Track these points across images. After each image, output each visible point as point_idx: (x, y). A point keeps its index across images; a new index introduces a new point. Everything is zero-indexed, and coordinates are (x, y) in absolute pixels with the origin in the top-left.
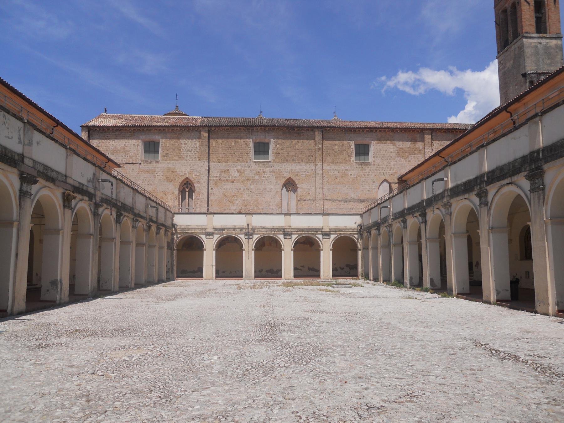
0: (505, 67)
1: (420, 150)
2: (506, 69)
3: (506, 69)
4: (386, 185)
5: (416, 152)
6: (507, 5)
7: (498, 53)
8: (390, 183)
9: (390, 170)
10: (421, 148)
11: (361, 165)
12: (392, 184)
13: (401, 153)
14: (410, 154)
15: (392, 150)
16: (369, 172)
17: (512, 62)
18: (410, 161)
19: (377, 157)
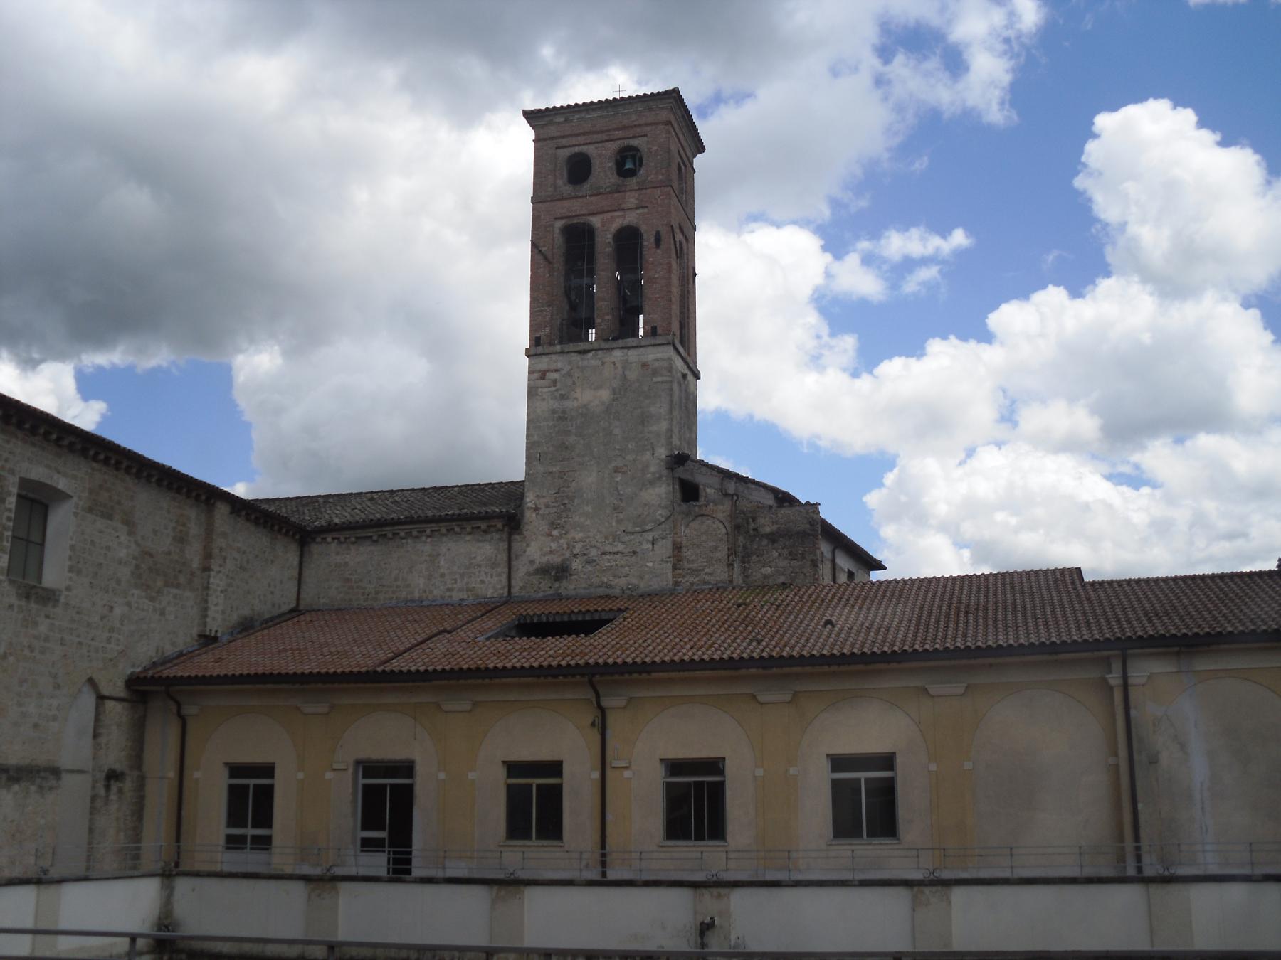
0: (563, 397)
1: (192, 574)
2: (569, 404)
3: (569, 404)
4: (88, 700)
5: (182, 579)
6: (596, 221)
7: (536, 341)
8: (101, 698)
9: (109, 640)
10: (195, 564)
11: (28, 597)
12: (110, 705)
13: (153, 574)
14: (166, 584)
15: (122, 553)
16: (47, 639)
17: (605, 395)
18: (162, 613)
19: (79, 572)
